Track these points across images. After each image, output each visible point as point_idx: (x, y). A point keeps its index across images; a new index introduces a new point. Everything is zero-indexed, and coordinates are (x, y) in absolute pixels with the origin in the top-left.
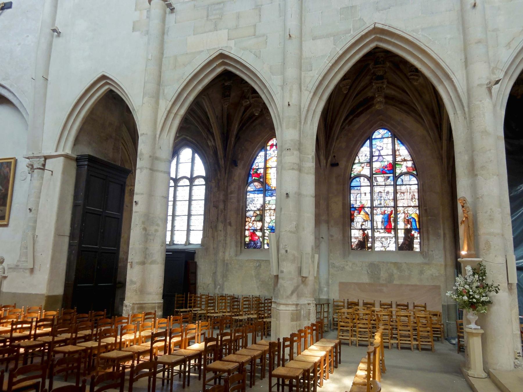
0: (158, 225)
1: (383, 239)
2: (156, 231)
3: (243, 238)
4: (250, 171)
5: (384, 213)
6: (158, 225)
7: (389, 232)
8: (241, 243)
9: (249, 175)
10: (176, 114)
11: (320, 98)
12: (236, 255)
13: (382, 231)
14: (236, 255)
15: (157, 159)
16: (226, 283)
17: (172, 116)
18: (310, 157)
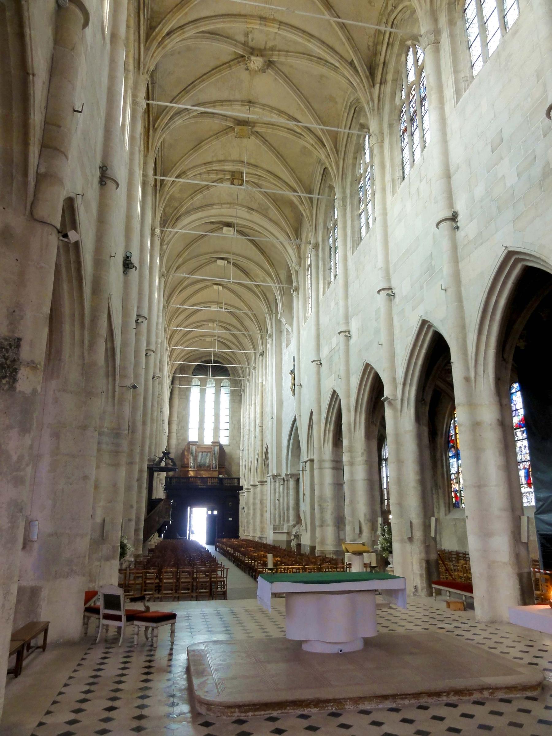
0: (328, 502)
1: (528, 494)
2: (328, 506)
3: (451, 499)
4: (448, 438)
5: (524, 468)
6: (328, 502)
7: (530, 487)
8: (449, 504)
9: (449, 442)
10: (329, 430)
11: (361, 412)
12: (446, 515)
13: (525, 486)
14: (446, 515)
15: (323, 461)
16: (442, 540)
17: (327, 432)
18: (360, 453)
